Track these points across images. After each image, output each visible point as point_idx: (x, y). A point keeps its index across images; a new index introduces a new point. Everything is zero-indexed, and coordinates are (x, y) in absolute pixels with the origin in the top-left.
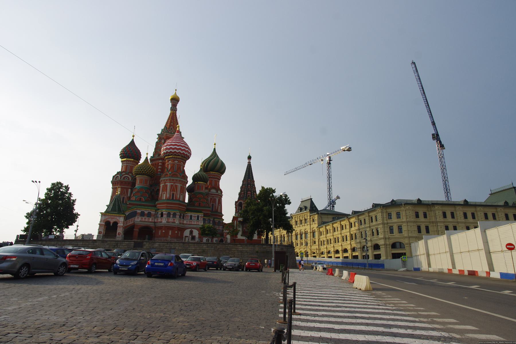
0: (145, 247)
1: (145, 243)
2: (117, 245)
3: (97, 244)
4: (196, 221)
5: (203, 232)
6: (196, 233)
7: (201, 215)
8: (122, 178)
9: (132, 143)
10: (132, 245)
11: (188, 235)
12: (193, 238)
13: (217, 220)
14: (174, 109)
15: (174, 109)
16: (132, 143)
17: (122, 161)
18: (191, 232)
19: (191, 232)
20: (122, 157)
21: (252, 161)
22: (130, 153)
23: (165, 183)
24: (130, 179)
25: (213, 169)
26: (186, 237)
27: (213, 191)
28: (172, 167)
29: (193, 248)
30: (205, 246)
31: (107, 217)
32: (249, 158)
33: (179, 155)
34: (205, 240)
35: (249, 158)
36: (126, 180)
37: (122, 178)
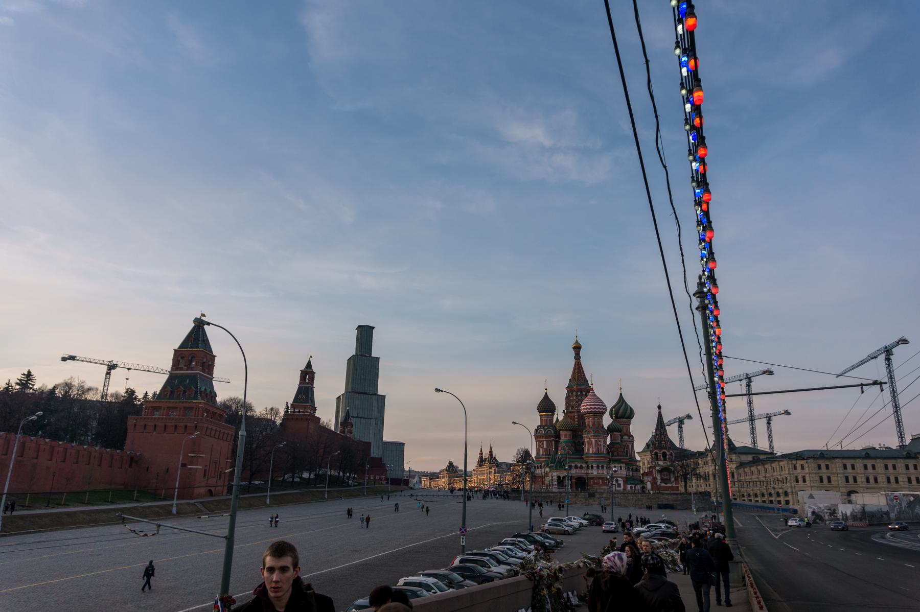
4: (619, 470)
5: (627, 480)
6: (621, 481)
7: (623, 465)
12: (619, 485)
13: (634, 468)
14: (577, 357)
15: (577, 357)
18: (617, 481)
20: (540, 412)
22: (546, 406)
25: (623, 417)
27: (626, 437)
28: (594, 424)
32: (659, 407)
34: (629, 486)
35: (659, 407)
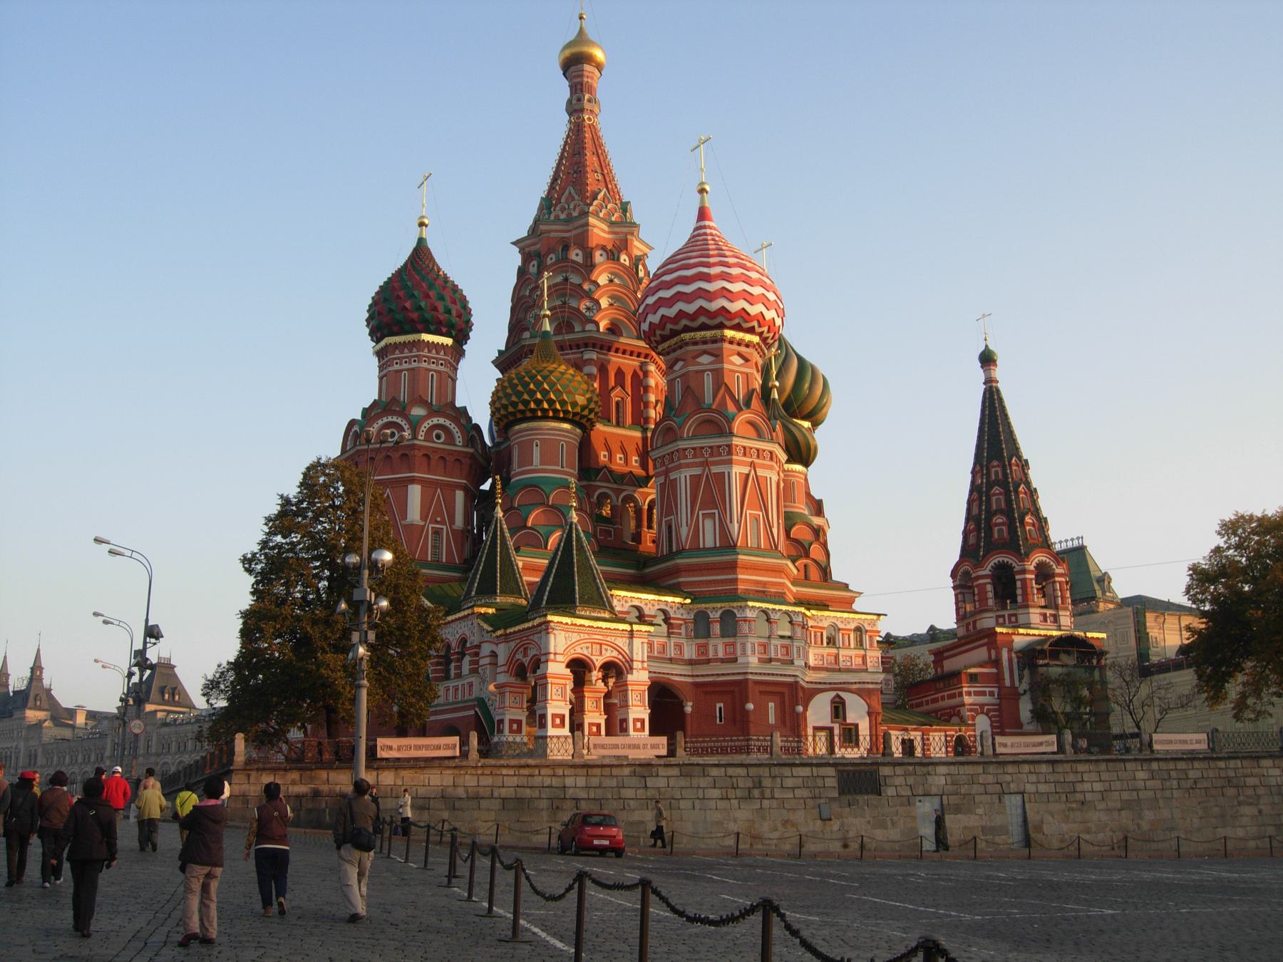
0: (891, 791)
1: (885, 771)
2: (759, 785)
3: (661, 783)
6: (857, 712)
8: (421, 435)
9: (421, 254)
10: (832, 782)
11: (827, 722)
12: (850, 735)
16: (421, 254)
17: (380, 354)
18: (838, 709)
19: (838, 709)
21: (1000, 372)
23: (706, 464)
24: (459, 440)
26: (816, 729)
29: (1098, 787)
30: (1141, 775)
31: (575, 637)
32: (987, 359)
33: (751, 330)
35: (987, 359)
36: (439, 444)
37: (421, 435)
